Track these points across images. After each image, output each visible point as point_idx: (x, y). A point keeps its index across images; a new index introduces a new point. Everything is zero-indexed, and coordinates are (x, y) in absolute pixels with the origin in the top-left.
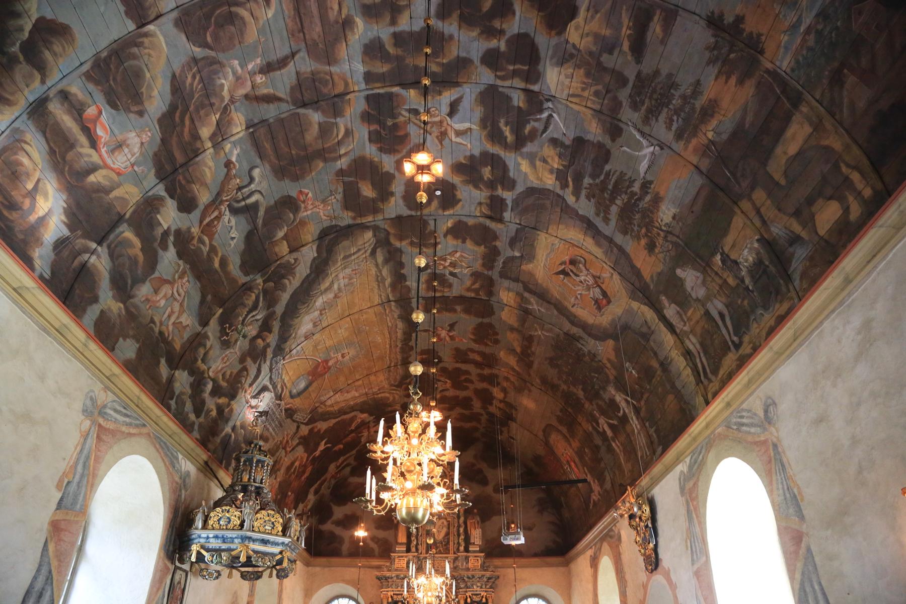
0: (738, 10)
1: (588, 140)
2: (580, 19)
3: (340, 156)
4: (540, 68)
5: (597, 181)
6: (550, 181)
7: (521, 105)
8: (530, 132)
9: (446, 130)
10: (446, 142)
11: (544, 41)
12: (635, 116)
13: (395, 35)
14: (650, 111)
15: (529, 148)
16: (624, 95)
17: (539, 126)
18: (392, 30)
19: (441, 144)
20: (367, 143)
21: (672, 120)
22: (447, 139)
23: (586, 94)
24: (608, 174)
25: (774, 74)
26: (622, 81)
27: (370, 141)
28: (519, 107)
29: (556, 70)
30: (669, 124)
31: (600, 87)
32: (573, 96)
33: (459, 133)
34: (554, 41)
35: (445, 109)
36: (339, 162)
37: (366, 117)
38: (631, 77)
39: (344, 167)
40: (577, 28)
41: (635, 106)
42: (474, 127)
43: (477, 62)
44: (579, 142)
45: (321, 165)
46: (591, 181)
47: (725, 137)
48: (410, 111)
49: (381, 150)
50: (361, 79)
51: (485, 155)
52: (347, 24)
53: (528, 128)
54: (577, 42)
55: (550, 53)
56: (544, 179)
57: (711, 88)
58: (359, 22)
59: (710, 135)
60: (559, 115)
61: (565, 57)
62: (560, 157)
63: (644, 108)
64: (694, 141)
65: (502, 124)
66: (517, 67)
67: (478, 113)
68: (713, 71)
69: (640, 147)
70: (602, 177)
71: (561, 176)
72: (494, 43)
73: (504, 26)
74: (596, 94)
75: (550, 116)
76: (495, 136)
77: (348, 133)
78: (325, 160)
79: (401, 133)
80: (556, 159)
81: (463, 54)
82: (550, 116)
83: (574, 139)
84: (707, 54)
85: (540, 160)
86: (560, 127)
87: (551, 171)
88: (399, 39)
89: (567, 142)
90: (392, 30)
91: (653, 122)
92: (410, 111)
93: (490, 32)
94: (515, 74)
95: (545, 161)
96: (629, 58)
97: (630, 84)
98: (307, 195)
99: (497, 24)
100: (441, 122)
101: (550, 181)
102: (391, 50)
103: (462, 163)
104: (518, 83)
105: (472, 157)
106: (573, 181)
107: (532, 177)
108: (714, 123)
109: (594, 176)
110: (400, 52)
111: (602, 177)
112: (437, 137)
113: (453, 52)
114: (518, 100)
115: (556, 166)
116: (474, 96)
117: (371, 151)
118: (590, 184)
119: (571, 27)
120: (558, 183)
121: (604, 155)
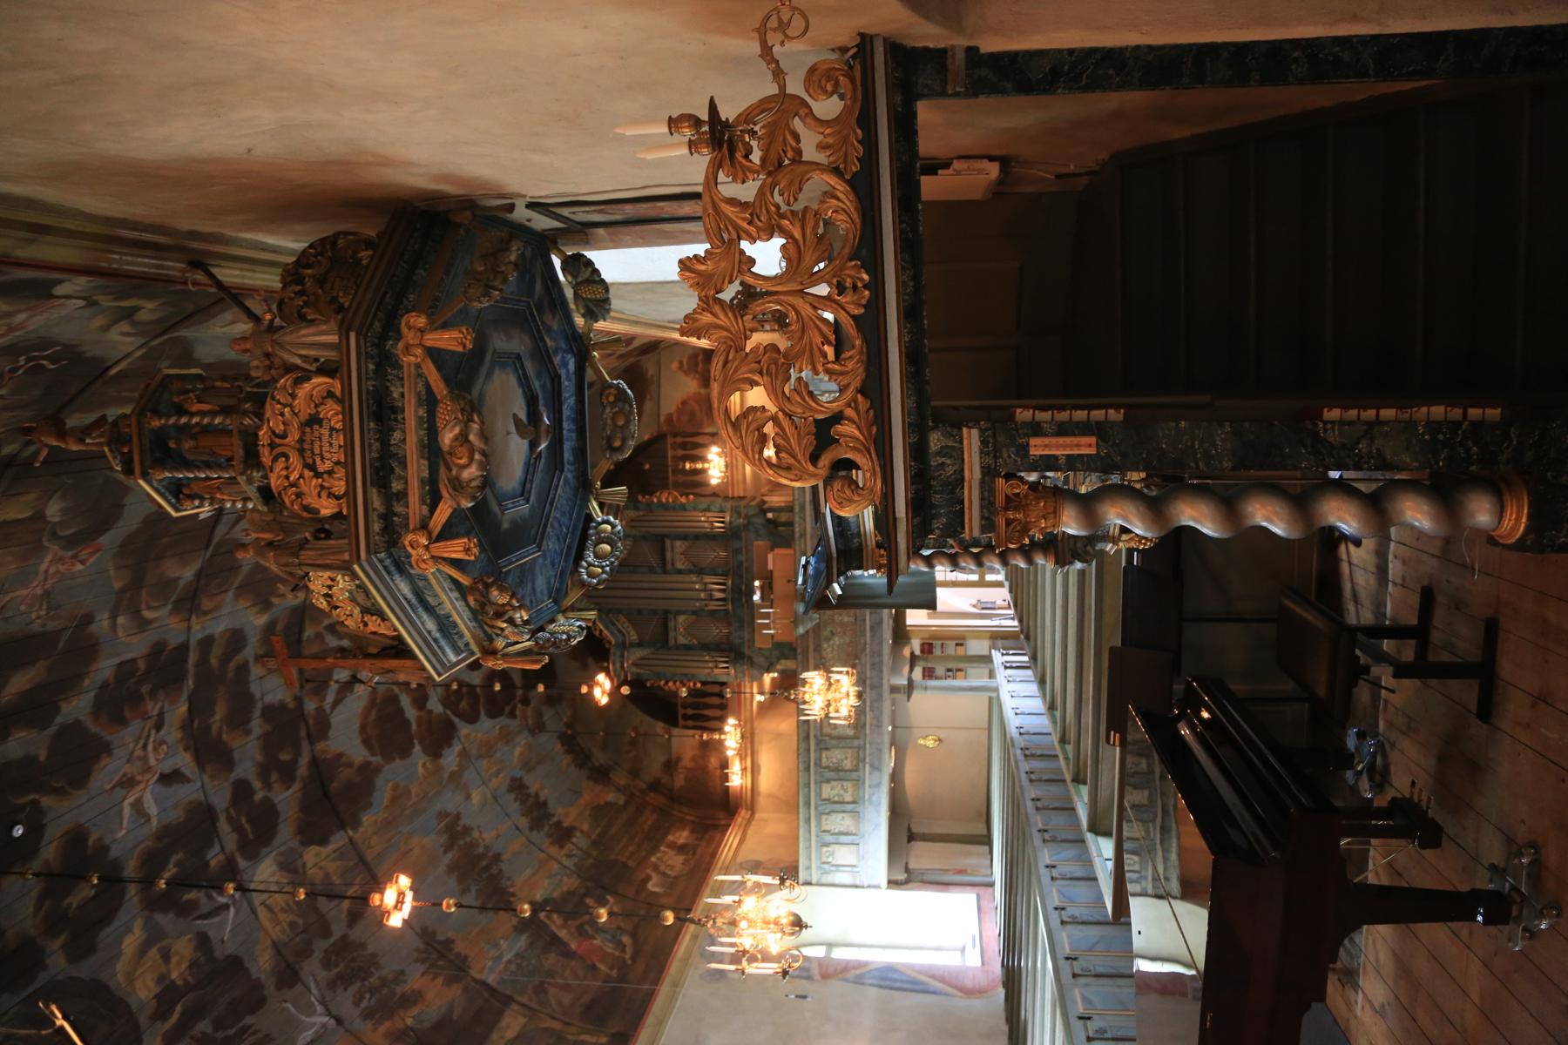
0: (450, 935)
1: (247, 970)
2: (326, 851)
3: (114, 617)
4: (264, 851)
5: (220, 1035)
6: (144, 991)
7: (213, 863)
8: (190, 902)
9: (139, 783)
10: (120, 792)
11: (286, 833)
12: (323, 975)
13: (246, 664)
14: (340, 977)
15: (165, 920)
16: (320, 946)
17: (205, 906)
18: (251, 660)
19: (114, 787)
20: (117, 661)
21: (362, 997)
22: (123, 792)
23: (282, 916)
24: (244, 1030)
25: (484, 984)
26: (326, 933)
27: (120, 665)
28: (207, 864)
29: (274, 868)
30: (357, 1002)
31: (300, 921)
32: (269, 908)
33: (137, 806)
34: (294, 844)
35: (167, 767)
36: (106, 615)
37: (158, 649)
38: (337, 935)
39: (93, 627)
40: (317, 855)
41: (327, 964)
42: (154, 822)
43: (234, 776)
44: (235, 964)
45: (117, 585)
46: (209, 1030)
47: (427, 1025)
48: (161, 714)
49: (105, 686)
50: (208, 632)
51: (116, 865)
52: (266, 605)
53: (192, 895)
54: (309, 865)
55: (282, 849)
56: (138, 984)
57: (415, 979)
58: (262, 620)
59: (409, 1022)
60: (237, 913)
61: (290, 866)
62: (190, 967)
63: (336, 971)
64: (387, 1024)
65: (175, 858)
66: (247, 826)
67: (176, 815)
68: (421, 968)
69: (309, 1010)
70: (232, 1032)
71: (168, 995)
72: (257, 785)
73: (276, 786)
74: (292, 925)
75: (226, 907)
76: (153, 861)
77: (143, 625)
78: (122, 591)
79: (127, 713)
80: (184, 966)
81: (236, 755)
82: (226, 907)
83: (229, 956)
84: (416, 955)
85: (160, 950)
86: (226, 930)
87: (161, 979)
88: (243, 669)
89: (219, 953)
90: (251, 660)
91: (340, 990)
92: (161, 714)
93: (264, 774)
94: (237, 828)
95: (166, 956)
96: (343, 916)
97: (332, 940)
98: (83, 562)
99: (274, 777)
100: (148, 769)
101: (144, 991)
102: (232, 665)
103: (86, 840)
104: (230, 840)
105: (103, 849)
106: (182, 1014)
107: (121, 967)
108: (415, 1011)
109: (219, 1024)
110: (230, 675)
111: (232, 1032)
112: (125, 775)
113: (235, 742)
114: (214, 858)
115: (174, 975)
116: (194, 796)
117: (104, 669)
118: (204, 1034)
119: (314, 849)
120: (154, 1003)
121: (255, 1000)
